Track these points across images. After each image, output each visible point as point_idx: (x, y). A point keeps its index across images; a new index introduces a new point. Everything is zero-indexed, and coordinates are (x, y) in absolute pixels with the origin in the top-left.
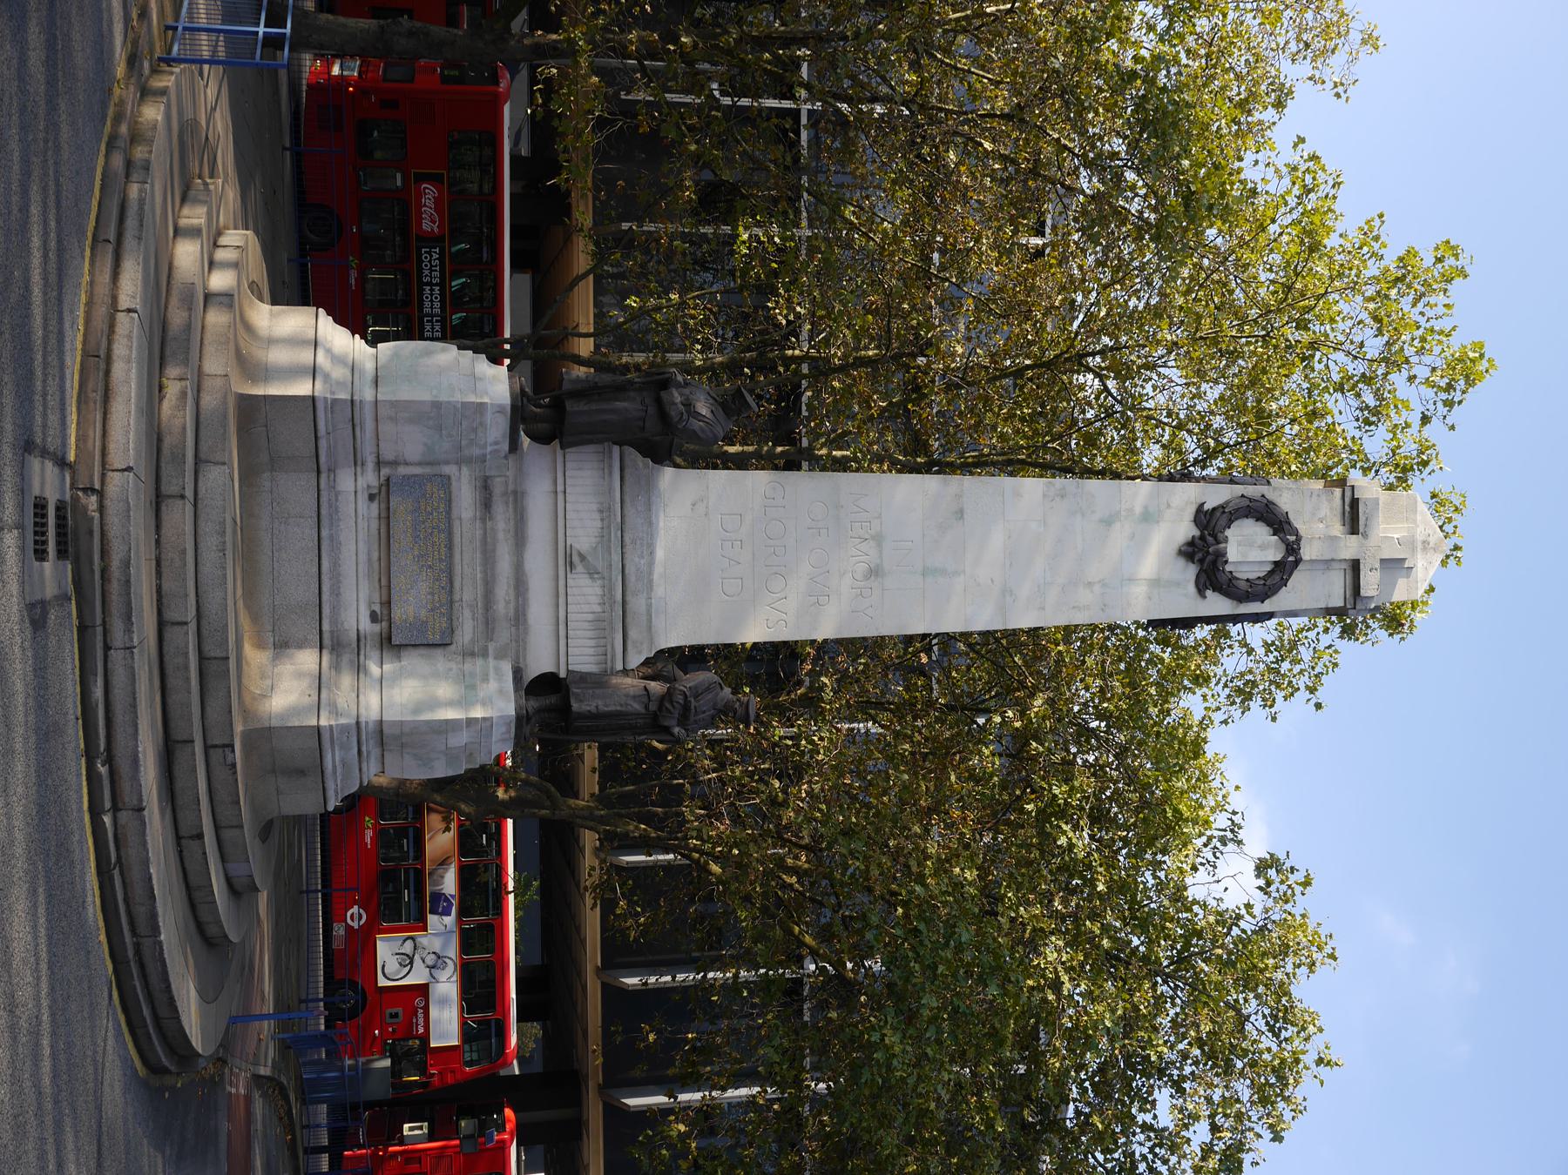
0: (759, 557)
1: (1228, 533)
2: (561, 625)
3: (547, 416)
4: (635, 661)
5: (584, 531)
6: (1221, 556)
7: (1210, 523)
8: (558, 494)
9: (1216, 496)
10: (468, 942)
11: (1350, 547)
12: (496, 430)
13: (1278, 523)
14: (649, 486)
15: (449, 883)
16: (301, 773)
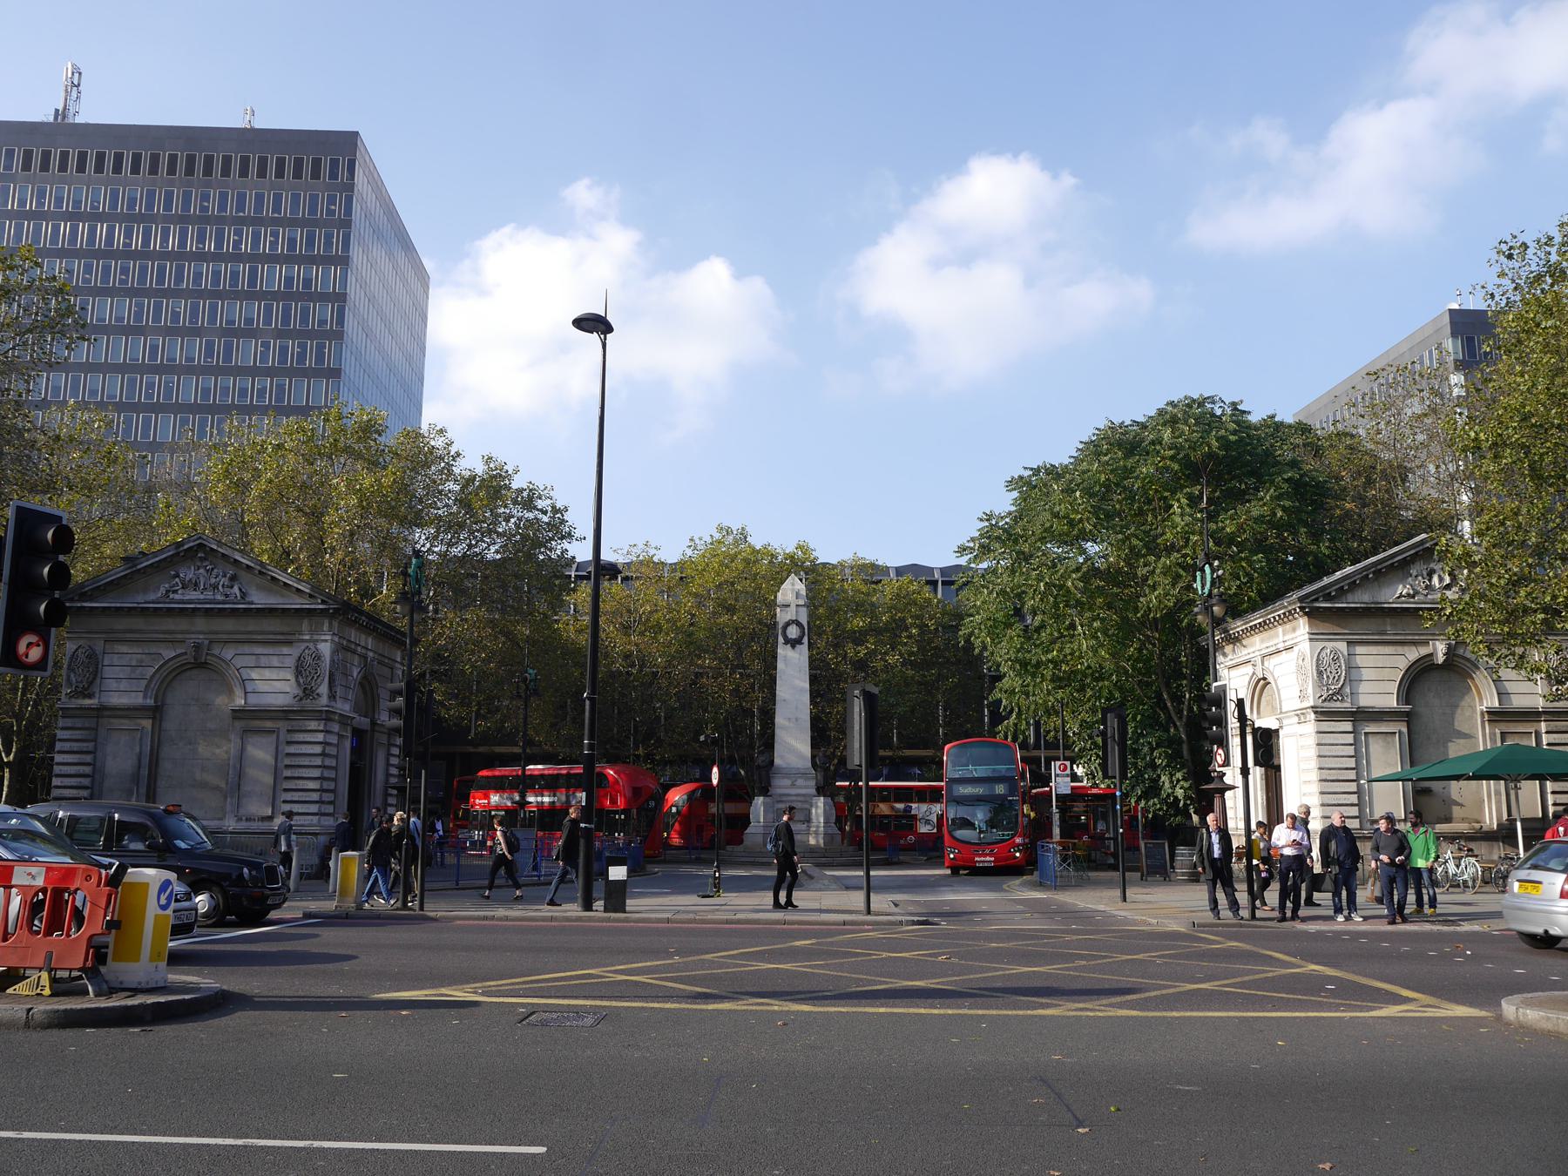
2: (806, 787)
3: (765, 791)
5: (787, 782)
7: (787, 641)
9: (781, 639)
10: (922, 800)
11: (793, 607)
14: (779, 768)
15: (900, 806)
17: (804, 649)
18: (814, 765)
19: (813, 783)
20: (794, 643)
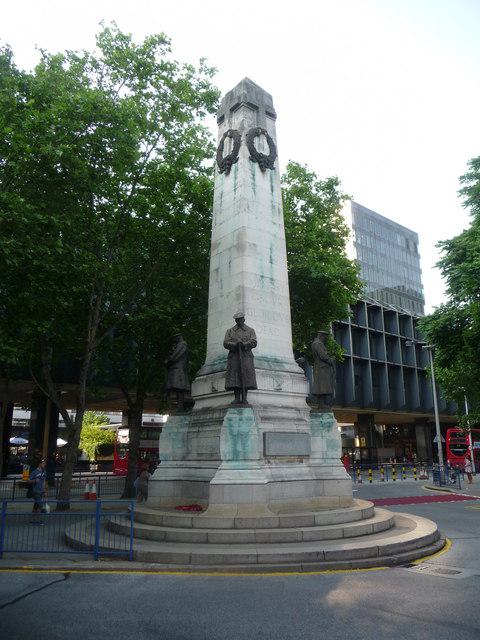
4: (301, 370)
7: (255, 157)
19: (303, 388)
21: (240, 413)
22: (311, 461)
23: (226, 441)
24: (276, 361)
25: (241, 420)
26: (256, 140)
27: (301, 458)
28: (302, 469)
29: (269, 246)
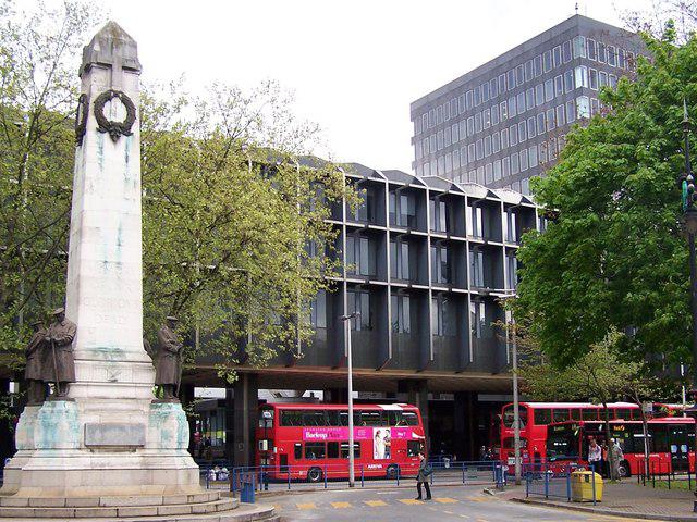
0: (106, 303)
1: (109, 120)
2: (136, 386)
6: (119, 125)
7: (105, 126)
8: (88, 385)
9: (92, 123)
12: (69, 405)
13: (107, 97)
16: (189, 475)
17: (131, 145)
18: (154, 346)
19: (149, 377)
20: (115, 131)
21: (54, 406)
22: (147, 452)
23: (39, 431)
24: (118, 352)
25: (53, 412)
26: (108, 104)
27: (133, 448)
28: (132, 459)
29: (117, 227)
